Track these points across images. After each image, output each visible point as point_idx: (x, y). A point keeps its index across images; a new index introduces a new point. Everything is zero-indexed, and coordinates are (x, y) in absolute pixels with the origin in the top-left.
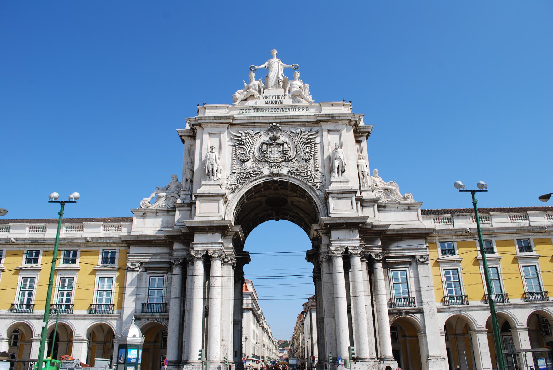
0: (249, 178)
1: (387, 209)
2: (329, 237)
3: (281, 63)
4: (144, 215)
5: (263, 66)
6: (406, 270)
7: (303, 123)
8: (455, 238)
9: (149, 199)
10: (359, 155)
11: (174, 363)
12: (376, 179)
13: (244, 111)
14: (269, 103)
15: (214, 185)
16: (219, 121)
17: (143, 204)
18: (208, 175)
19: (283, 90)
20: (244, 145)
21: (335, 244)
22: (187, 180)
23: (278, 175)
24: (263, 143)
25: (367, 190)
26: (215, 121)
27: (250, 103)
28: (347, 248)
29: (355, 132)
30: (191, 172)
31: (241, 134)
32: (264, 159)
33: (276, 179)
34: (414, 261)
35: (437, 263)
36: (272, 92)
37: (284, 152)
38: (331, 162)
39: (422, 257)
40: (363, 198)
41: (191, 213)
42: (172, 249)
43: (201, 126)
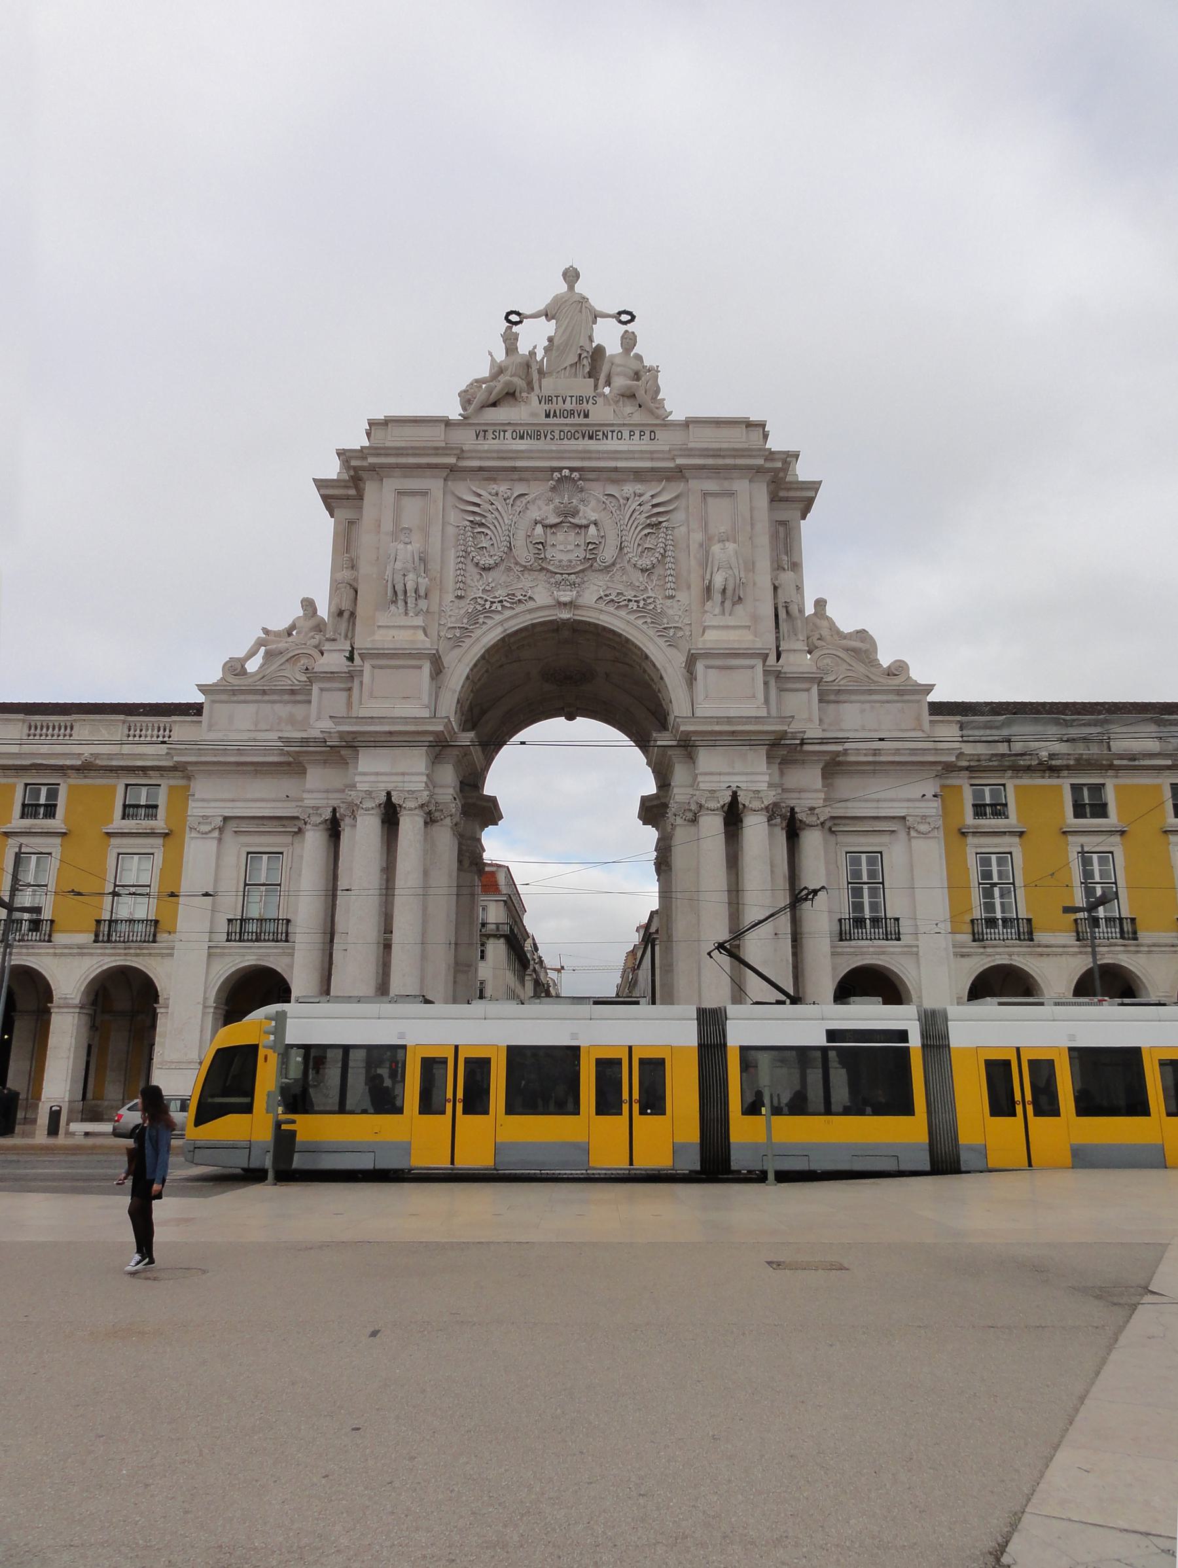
1: (842, 698)
7: (639, 475)
8: (1012, 778)
18: (394, 602)
22: (340, 613)
28: (735, 795)
29: (774, 499)
33: (565, 615)
38: (708, 577)
39: (924, 817)
41: (350, 697)
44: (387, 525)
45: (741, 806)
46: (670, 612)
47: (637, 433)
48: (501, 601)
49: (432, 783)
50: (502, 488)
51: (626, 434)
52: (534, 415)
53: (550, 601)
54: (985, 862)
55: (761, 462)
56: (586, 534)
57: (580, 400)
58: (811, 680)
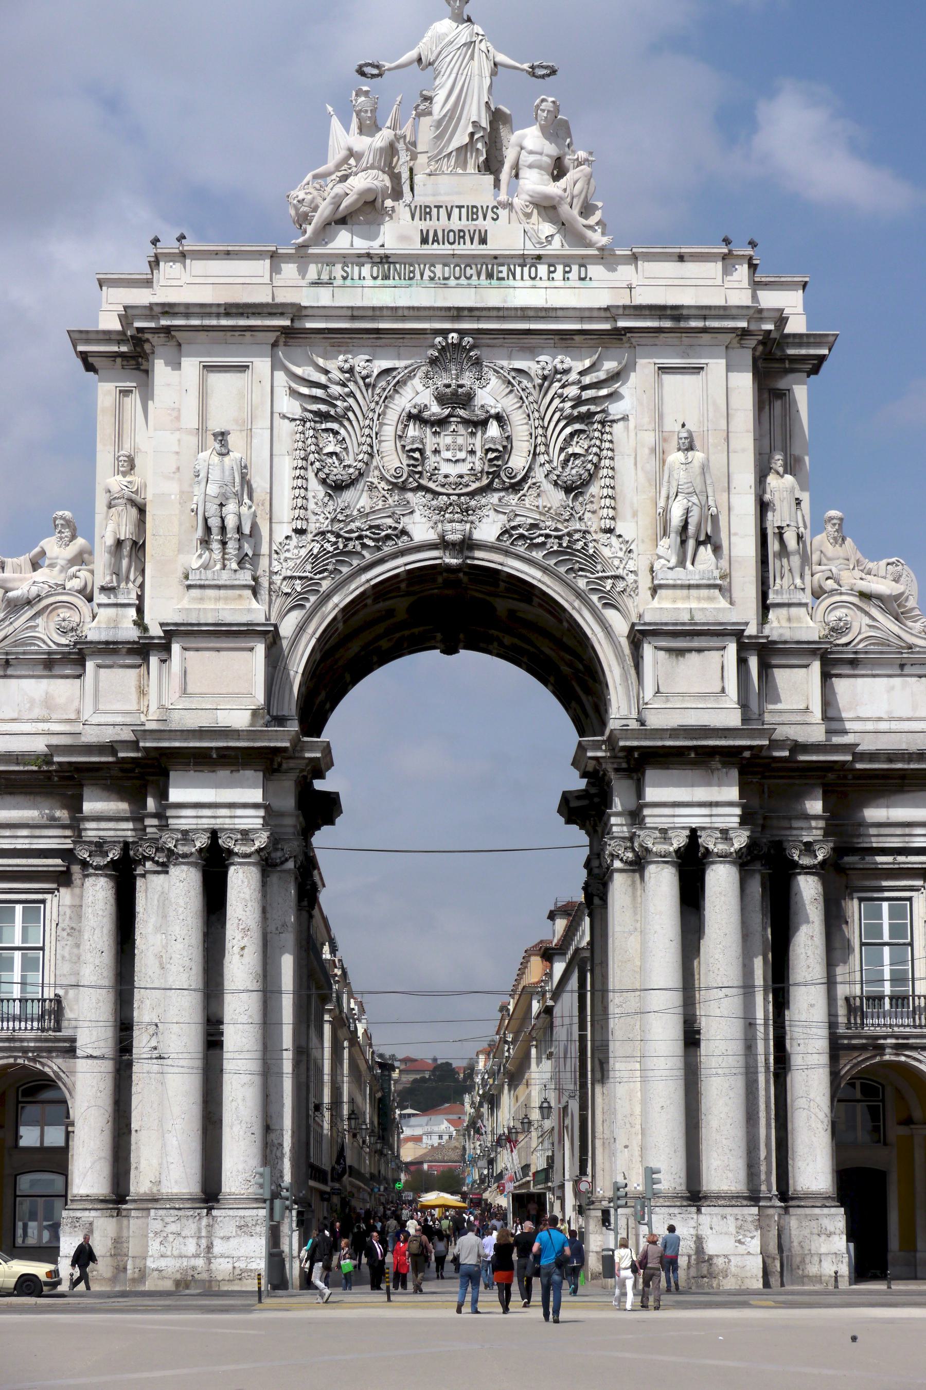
2: (640, 794)
6: (910, 899)
11: (102, 1201)
13: (338, 271)
14: (436, 240)
15: (233, 587)
16: (242, 322)
21: (653, 818)
22: (119, 543)
23: (467, 545)
24: (410, 416)
25: (789, 605)
26: (224, 322)
30: (134, 512)
31: (326, 372)
33: (452, 561)
38: (662, 503)
40: (775, 637)
42: (80, 810)
43: (173, 337)
44: (191, 420)
45: (702, 850)
46: (606, 552)
47: (560, 268)
48: (360, 538)
49: (271, 814)
51: (543, 269)
52: (403, 238)
53: (431, 536)
55: (744, 324)
56: (484, 433)
57: (473, 212)
58: (813, 653)
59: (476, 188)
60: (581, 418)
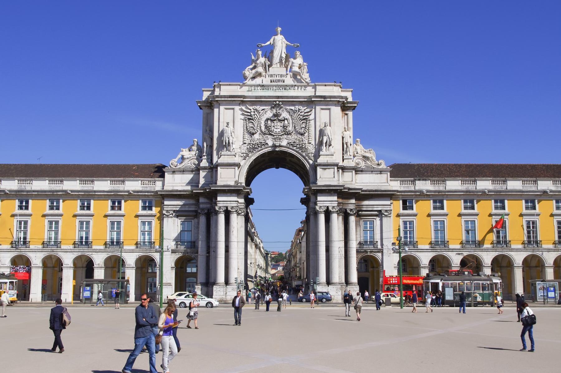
0: (256, 148)
2: (316, 199)
3: (284, 40)
4: (174, 172)
5: (268, 43)
9: (176, 160)
10: (345, 128)
12: (358, 147)
13: (253, 88)
17: (172, 164)
18: (225, 146)
19: (285, 69)
20: (252, 119)
21: (319, 204)
23: (280, 146)
27: (258, 81)
28: (328, 207)
32: (268, 132)
33: (277, 149)
34: (380, 214)
35: (398, 216)
36: (277, 69)
37: (284, 127)
39: (386, 211)
42: (199, 202)
50: (258, 107)
51: (296, 88)
54: (405, 223)
57: (281, 76)
59: (283, 71)
60: (304, 119)
